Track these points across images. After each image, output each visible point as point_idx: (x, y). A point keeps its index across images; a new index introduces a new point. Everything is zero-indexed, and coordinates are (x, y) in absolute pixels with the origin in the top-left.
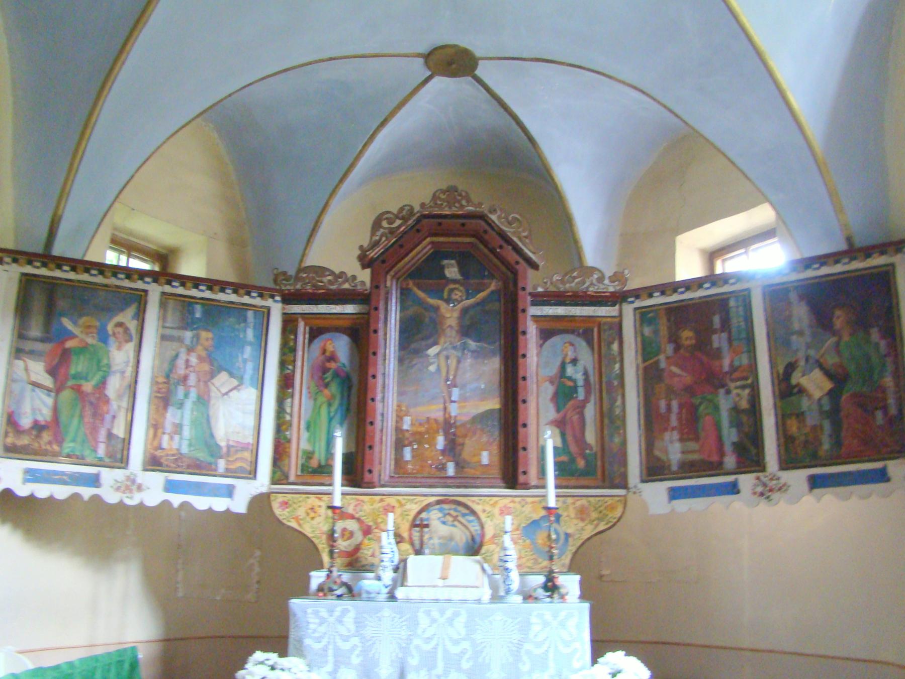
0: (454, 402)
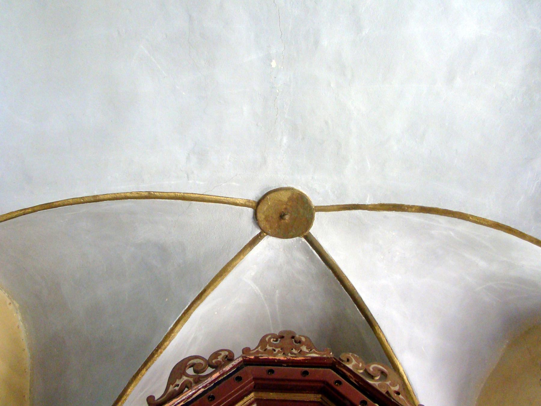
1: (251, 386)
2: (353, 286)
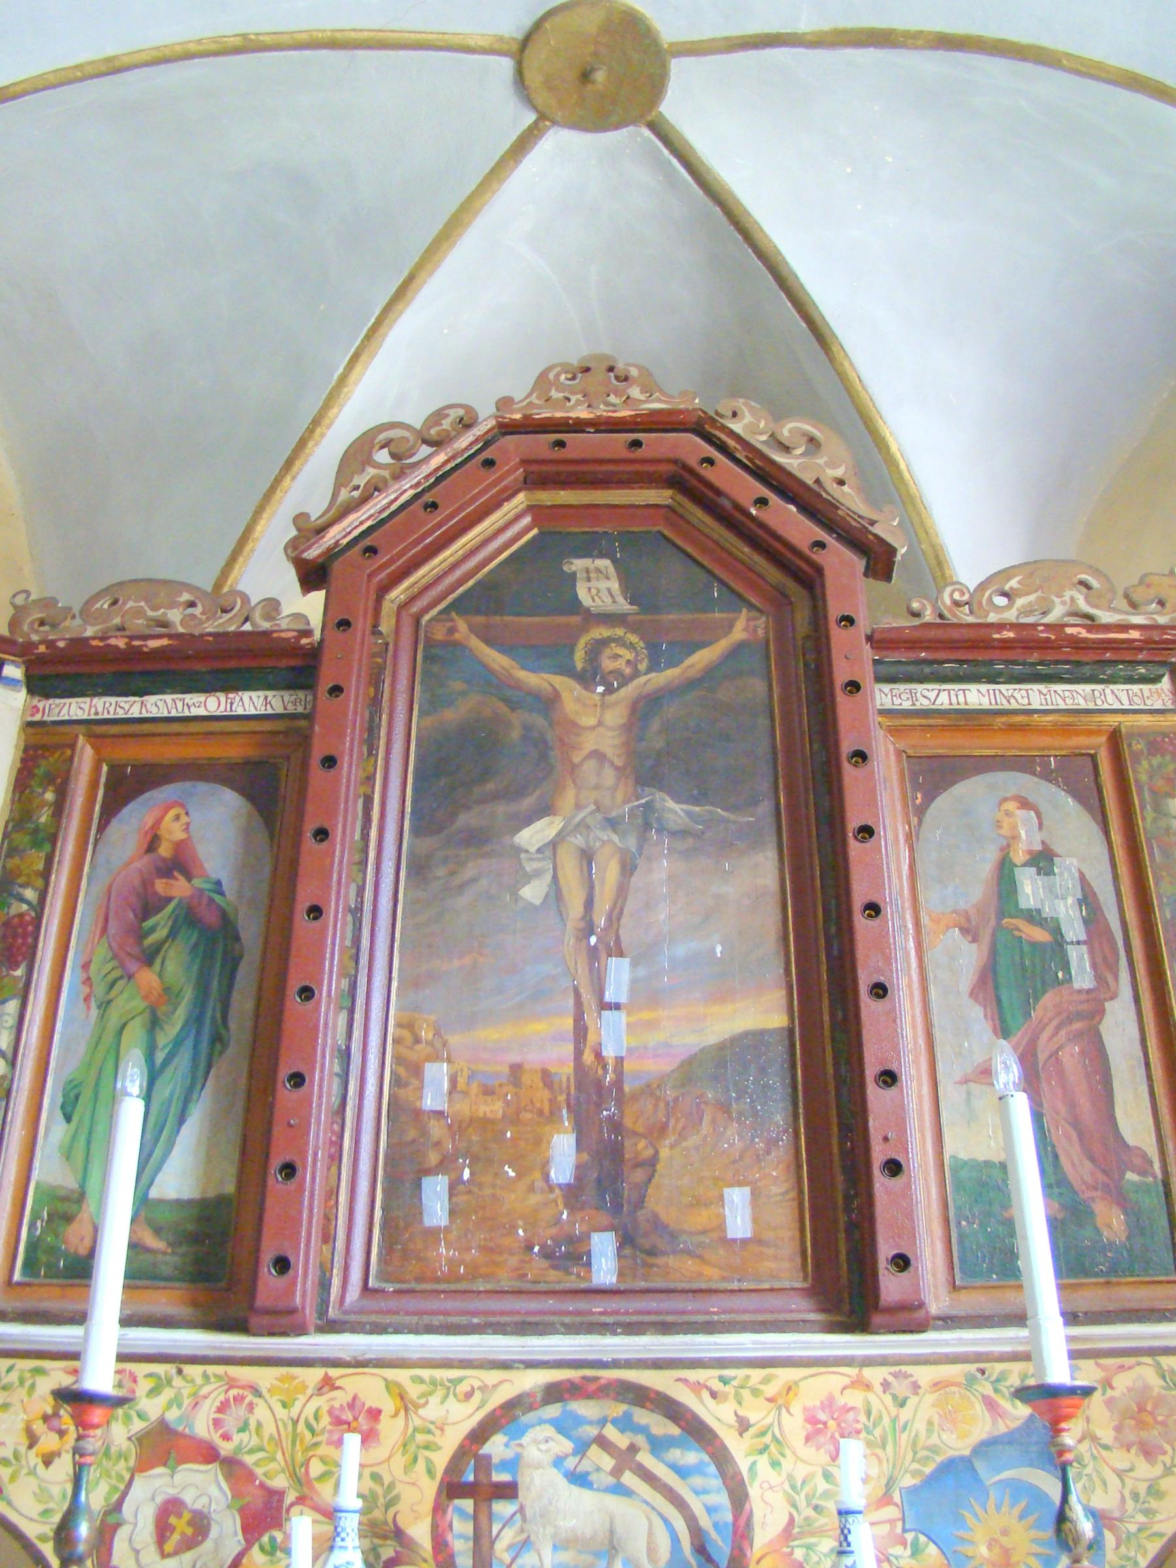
0: (617, 1007)
1: (516, 480)
2: (775, 247)
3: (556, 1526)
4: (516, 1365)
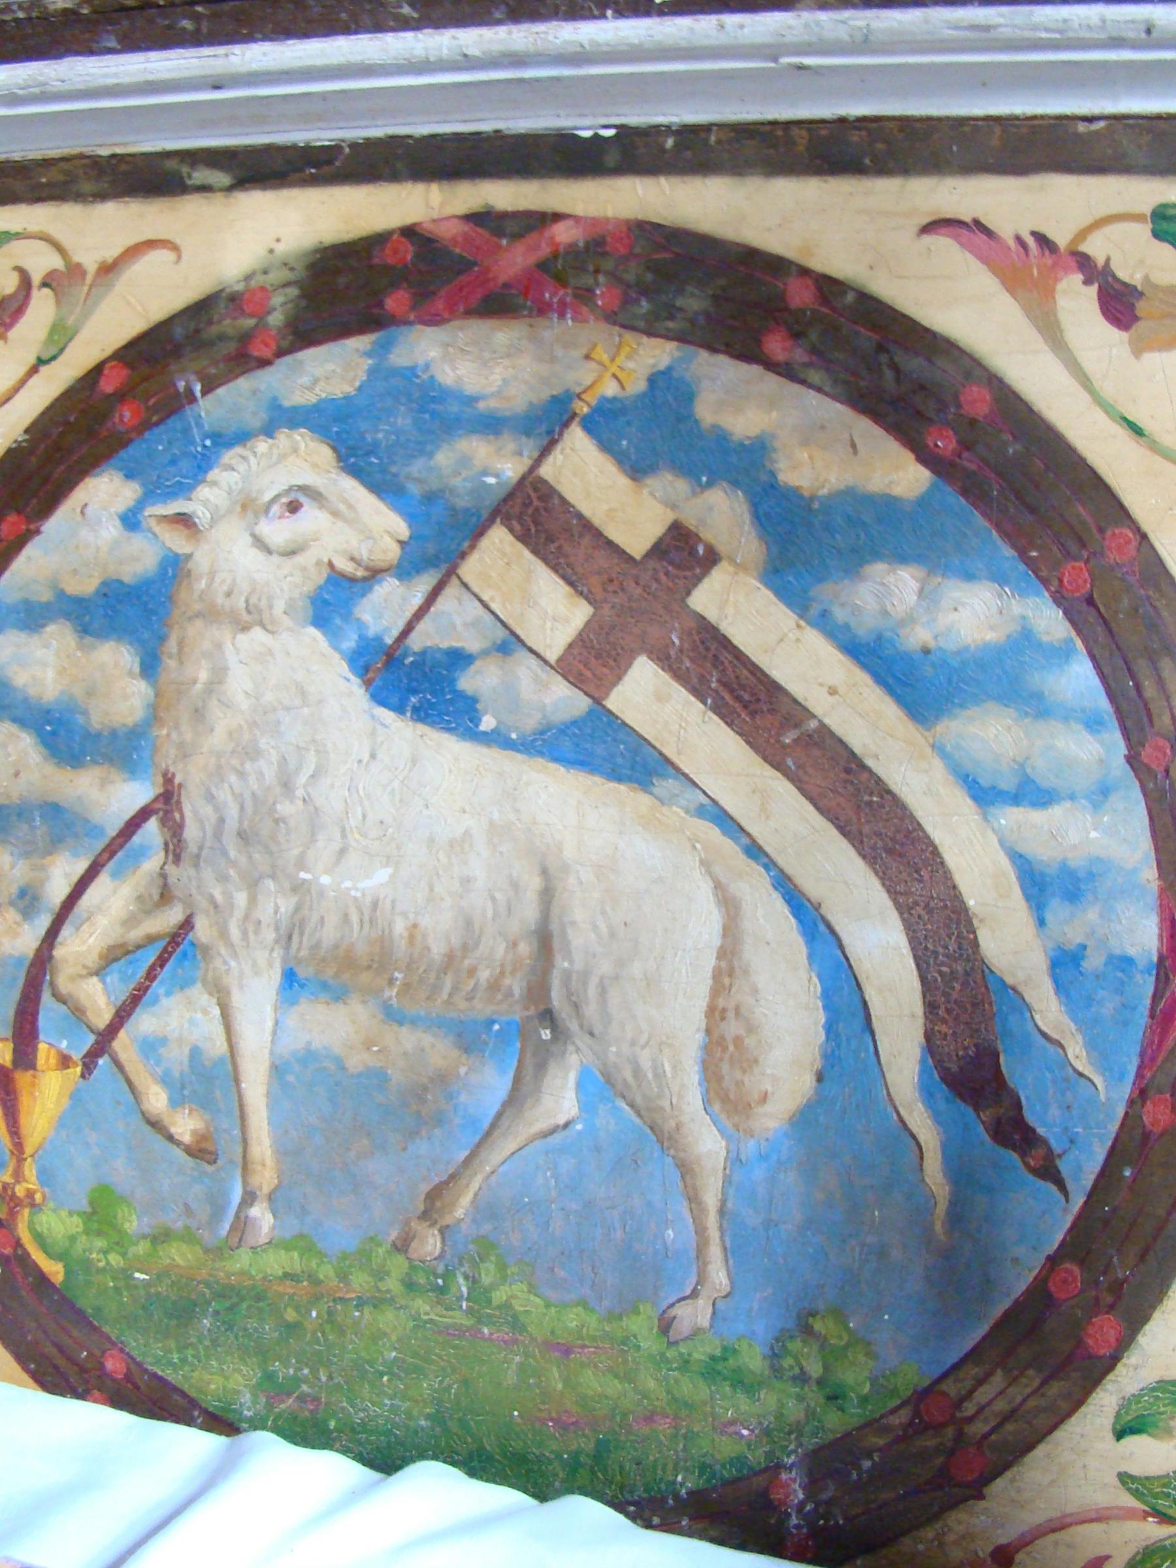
3: (298, 888)
4: (201, 175)
